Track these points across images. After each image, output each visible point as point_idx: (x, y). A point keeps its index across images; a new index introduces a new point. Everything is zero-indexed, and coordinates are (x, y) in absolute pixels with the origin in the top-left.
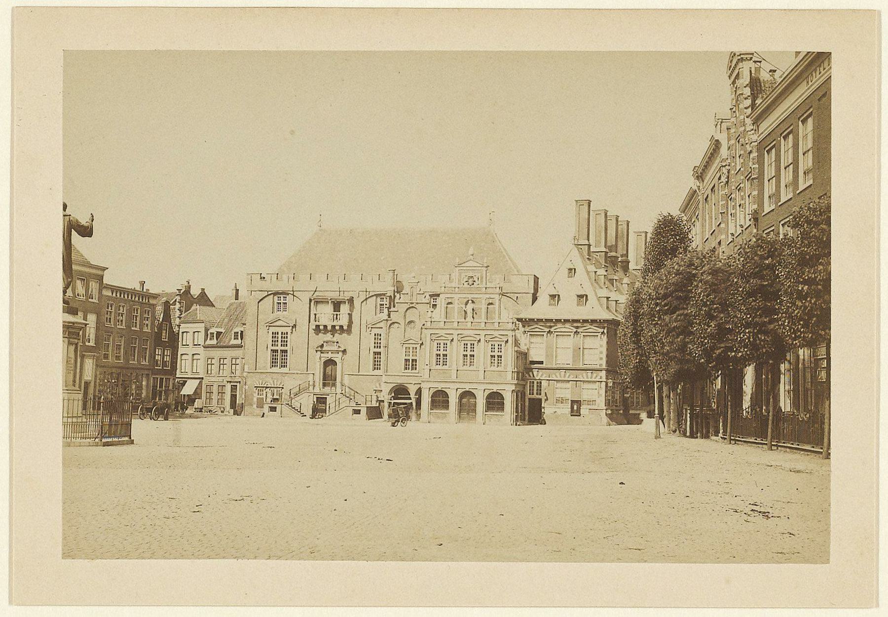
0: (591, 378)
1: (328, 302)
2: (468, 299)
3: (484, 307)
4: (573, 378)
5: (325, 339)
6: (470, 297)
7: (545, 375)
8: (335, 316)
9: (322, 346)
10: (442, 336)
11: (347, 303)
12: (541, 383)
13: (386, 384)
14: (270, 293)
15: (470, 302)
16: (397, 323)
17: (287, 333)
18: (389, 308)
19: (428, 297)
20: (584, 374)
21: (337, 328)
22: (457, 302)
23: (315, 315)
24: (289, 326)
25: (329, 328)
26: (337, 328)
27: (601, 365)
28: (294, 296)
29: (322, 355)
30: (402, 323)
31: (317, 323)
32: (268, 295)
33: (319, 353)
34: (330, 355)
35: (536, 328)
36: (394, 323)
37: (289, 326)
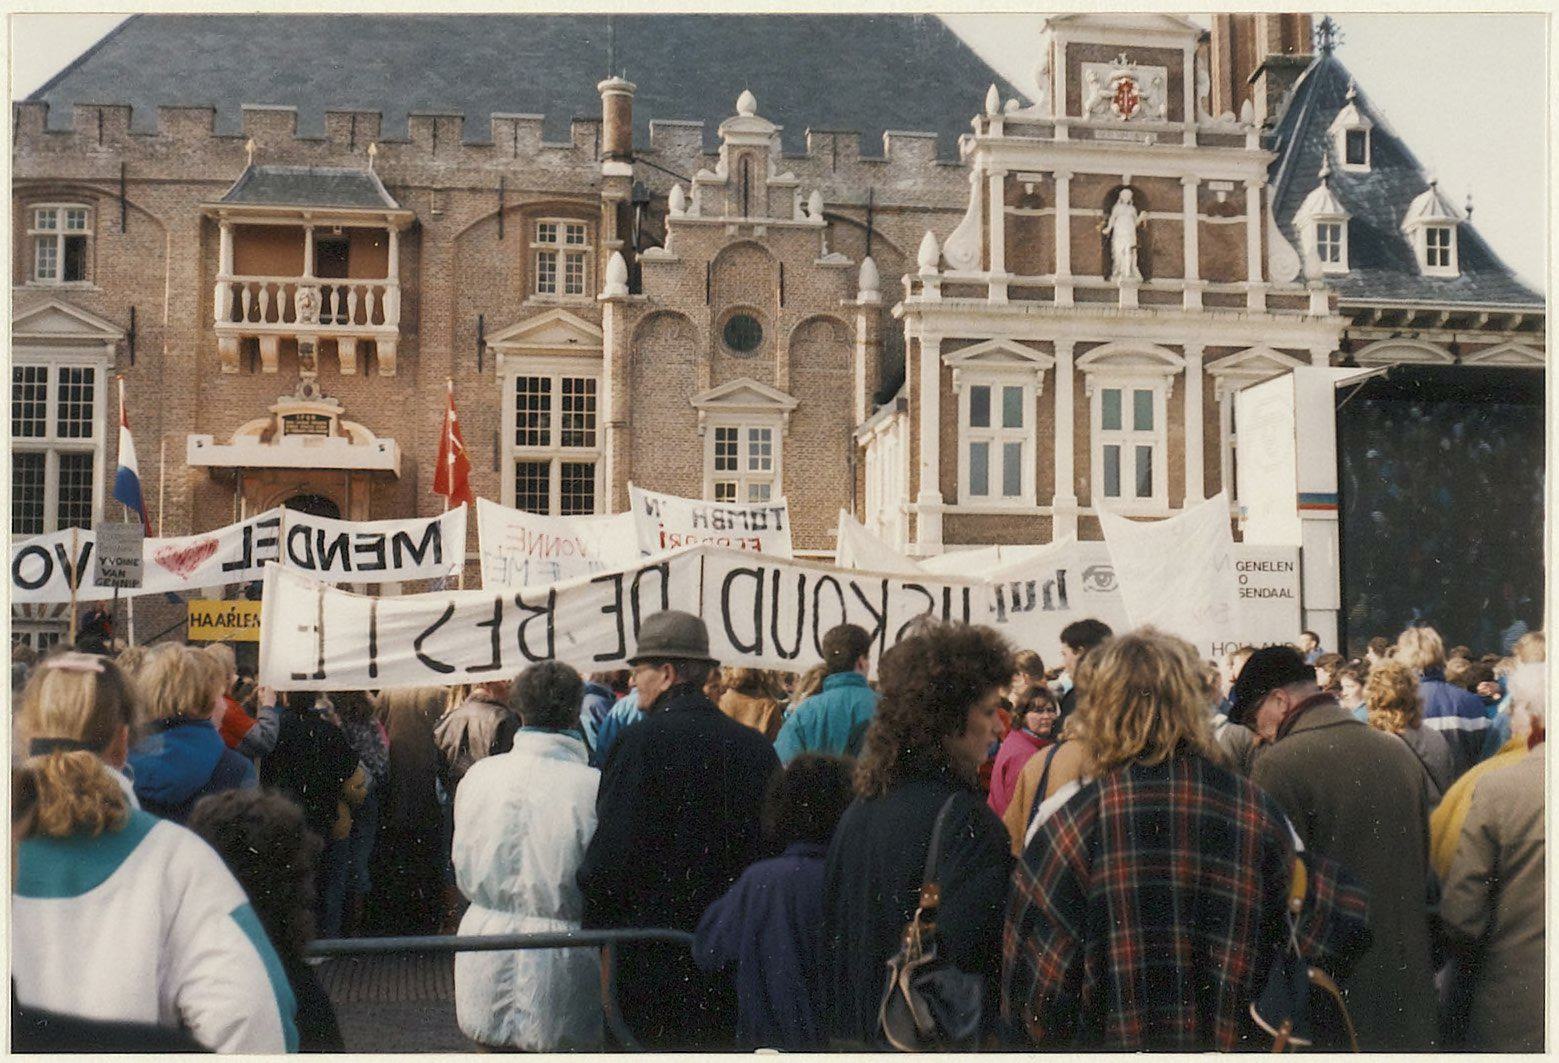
2: (1115, 184)
3: (1191, 218)
6: (1127, 168)
8: (334, 299)
10: (1000, 351)
15: (1126, 195)
16: (670, 314)
17: (90, 373)
18: (627, 253)
19: (815, 202)
21: (347, 350)
22: (1062, 189)
23: (237, 289)
24: (103, 343)
26: (347, 350)
30: (700, 316)
31: (247, 326)
36: (656, 316)
37: (103, 343)
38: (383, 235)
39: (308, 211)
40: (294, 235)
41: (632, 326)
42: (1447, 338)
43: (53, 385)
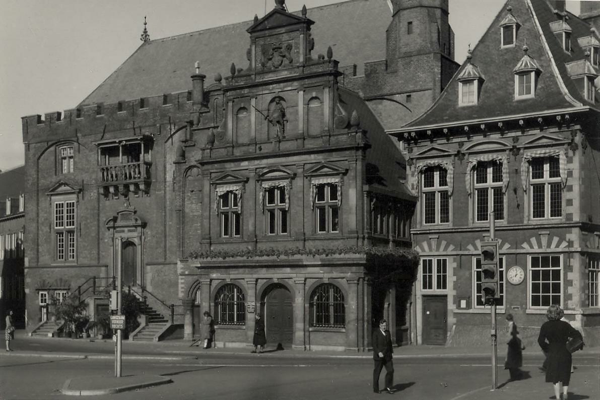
0: (549, 246)
1: (118, 148)
4: (509, 248)
5: (122, 209)
7: (451, 247)
9: (115, 219)
11: (142, 145)
12: (445, 261)
13: (184, 277)
14: (50, 143)
20: (533, 240)
27: (569, 216)
28: (79, 143)
29: (117, 235)
32: (49, 147)
33: (112, 230)
35: (433, 149)
36: (191, 167)
38: (139, 145)
40: (118, 148)
41: (183, 171)
43: (65, 209)
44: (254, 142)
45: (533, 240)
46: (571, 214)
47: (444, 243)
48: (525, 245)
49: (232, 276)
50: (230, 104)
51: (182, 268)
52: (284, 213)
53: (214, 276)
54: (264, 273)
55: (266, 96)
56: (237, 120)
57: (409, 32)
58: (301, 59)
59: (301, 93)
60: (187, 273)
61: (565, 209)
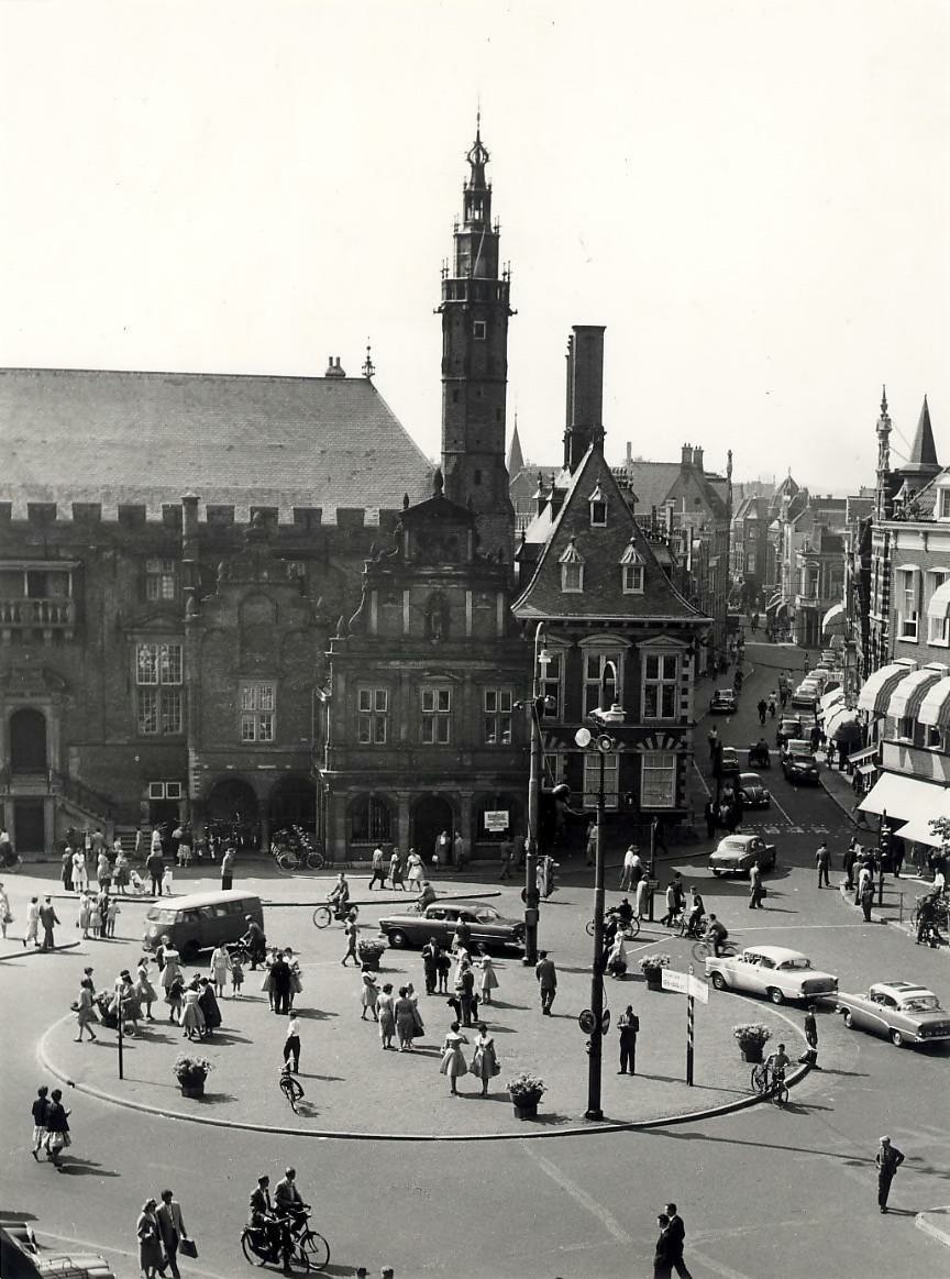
1: (22, 572)
7: (563, 744)
20: (649, 740)
25: (27, 634)
34: (27, 701)
36: (213, 630)
39: (26, 564)
40: (22, 572)
42: (630, 632)
44: (408, 639)
45: (649, 740)
46: (686, 717)
47: (554, 740)
48: (640, 745)
49: (377, 789)
50: (374, 593)
51: (196, 761)
52: (443, 722)
53: (352, 788)
54: (423, 788)
55: (425, 591)
56: (381, 611)
57: (478, 481)
58: (470, 557)
59: (469, 594)
60: (206, 767)
61: (679, 712)
